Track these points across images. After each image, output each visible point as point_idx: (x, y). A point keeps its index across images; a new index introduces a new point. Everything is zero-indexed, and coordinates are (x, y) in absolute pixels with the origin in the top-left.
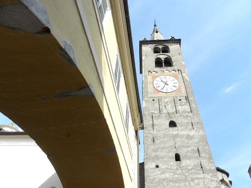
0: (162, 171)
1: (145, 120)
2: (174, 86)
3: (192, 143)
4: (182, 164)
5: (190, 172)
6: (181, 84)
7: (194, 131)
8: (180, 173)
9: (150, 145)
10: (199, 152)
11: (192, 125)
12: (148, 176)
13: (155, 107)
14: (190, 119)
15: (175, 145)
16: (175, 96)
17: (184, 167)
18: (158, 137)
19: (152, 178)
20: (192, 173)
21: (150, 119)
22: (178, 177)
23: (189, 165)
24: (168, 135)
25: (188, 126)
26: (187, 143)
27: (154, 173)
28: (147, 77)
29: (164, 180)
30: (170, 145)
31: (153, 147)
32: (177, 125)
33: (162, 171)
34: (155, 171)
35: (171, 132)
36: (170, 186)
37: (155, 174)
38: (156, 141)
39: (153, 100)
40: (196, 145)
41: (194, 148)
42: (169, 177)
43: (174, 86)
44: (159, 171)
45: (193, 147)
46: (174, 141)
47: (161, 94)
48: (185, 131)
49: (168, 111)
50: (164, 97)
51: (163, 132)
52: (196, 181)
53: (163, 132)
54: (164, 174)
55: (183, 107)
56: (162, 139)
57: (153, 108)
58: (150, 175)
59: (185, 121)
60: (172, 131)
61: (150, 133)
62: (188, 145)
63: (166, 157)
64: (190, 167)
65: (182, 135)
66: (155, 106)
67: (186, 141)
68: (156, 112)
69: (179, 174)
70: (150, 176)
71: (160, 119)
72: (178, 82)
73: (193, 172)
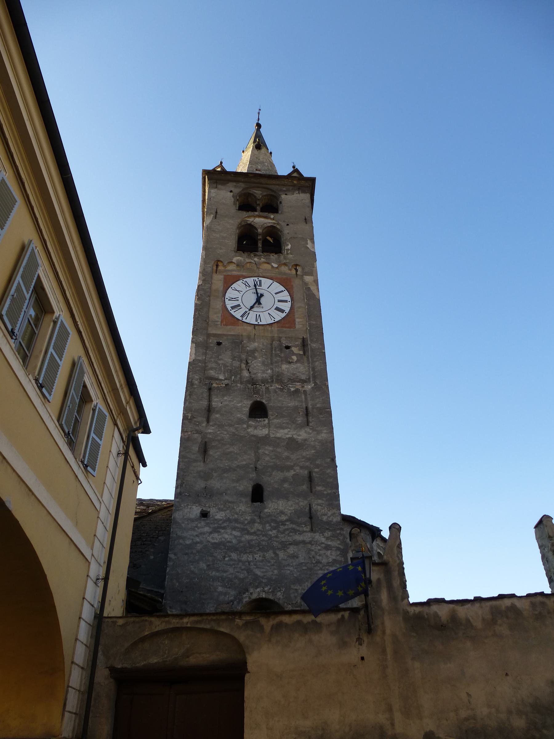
2: (277, 309)
3: (298, 459)
4: (266, 510)
5: (282, 528)
6: (297, 305)
7: (308, 429)
8: (258, 530)
12: (180, 537)
13: (220, 362)
14: (304, 400)
17: (269, 516)
19: (188, 542)
22: (252, 540)
23: (282, 513)
25: (296, 417)
26: (288, 458)
27: (194, 530)
28: (212, 277)
29: (216, 546)
30: (244, 463)
31: (200, 466)
33: (216, 525)
34: (197, 527)
36: (228, 560)
37: (195, 533)
38: (211, 452)
39: (219, 344)
40: (308, 464)
41: (301, 471)
44: (207, 525)
45: (298, 469)
47: (240, 327)
48: (286, 428)
50: (249, 337)
51: (232, 430)
52: (292, 550)
53: (232, 430)
54: (219, 532)
55: (293, 366)
57: (214, 365)
58: (185, 534)
60: (256, 428)
61: (198, 432)
62: (288, 463)
63: (229, 492)
64: (284, 518)
65: (279, 438)
66: (221, 359)
67: (286, 454)
68: (221, 377)
69: (254, 533)
70: (184, 538)
72: (289, 298)
73: (287, 529)
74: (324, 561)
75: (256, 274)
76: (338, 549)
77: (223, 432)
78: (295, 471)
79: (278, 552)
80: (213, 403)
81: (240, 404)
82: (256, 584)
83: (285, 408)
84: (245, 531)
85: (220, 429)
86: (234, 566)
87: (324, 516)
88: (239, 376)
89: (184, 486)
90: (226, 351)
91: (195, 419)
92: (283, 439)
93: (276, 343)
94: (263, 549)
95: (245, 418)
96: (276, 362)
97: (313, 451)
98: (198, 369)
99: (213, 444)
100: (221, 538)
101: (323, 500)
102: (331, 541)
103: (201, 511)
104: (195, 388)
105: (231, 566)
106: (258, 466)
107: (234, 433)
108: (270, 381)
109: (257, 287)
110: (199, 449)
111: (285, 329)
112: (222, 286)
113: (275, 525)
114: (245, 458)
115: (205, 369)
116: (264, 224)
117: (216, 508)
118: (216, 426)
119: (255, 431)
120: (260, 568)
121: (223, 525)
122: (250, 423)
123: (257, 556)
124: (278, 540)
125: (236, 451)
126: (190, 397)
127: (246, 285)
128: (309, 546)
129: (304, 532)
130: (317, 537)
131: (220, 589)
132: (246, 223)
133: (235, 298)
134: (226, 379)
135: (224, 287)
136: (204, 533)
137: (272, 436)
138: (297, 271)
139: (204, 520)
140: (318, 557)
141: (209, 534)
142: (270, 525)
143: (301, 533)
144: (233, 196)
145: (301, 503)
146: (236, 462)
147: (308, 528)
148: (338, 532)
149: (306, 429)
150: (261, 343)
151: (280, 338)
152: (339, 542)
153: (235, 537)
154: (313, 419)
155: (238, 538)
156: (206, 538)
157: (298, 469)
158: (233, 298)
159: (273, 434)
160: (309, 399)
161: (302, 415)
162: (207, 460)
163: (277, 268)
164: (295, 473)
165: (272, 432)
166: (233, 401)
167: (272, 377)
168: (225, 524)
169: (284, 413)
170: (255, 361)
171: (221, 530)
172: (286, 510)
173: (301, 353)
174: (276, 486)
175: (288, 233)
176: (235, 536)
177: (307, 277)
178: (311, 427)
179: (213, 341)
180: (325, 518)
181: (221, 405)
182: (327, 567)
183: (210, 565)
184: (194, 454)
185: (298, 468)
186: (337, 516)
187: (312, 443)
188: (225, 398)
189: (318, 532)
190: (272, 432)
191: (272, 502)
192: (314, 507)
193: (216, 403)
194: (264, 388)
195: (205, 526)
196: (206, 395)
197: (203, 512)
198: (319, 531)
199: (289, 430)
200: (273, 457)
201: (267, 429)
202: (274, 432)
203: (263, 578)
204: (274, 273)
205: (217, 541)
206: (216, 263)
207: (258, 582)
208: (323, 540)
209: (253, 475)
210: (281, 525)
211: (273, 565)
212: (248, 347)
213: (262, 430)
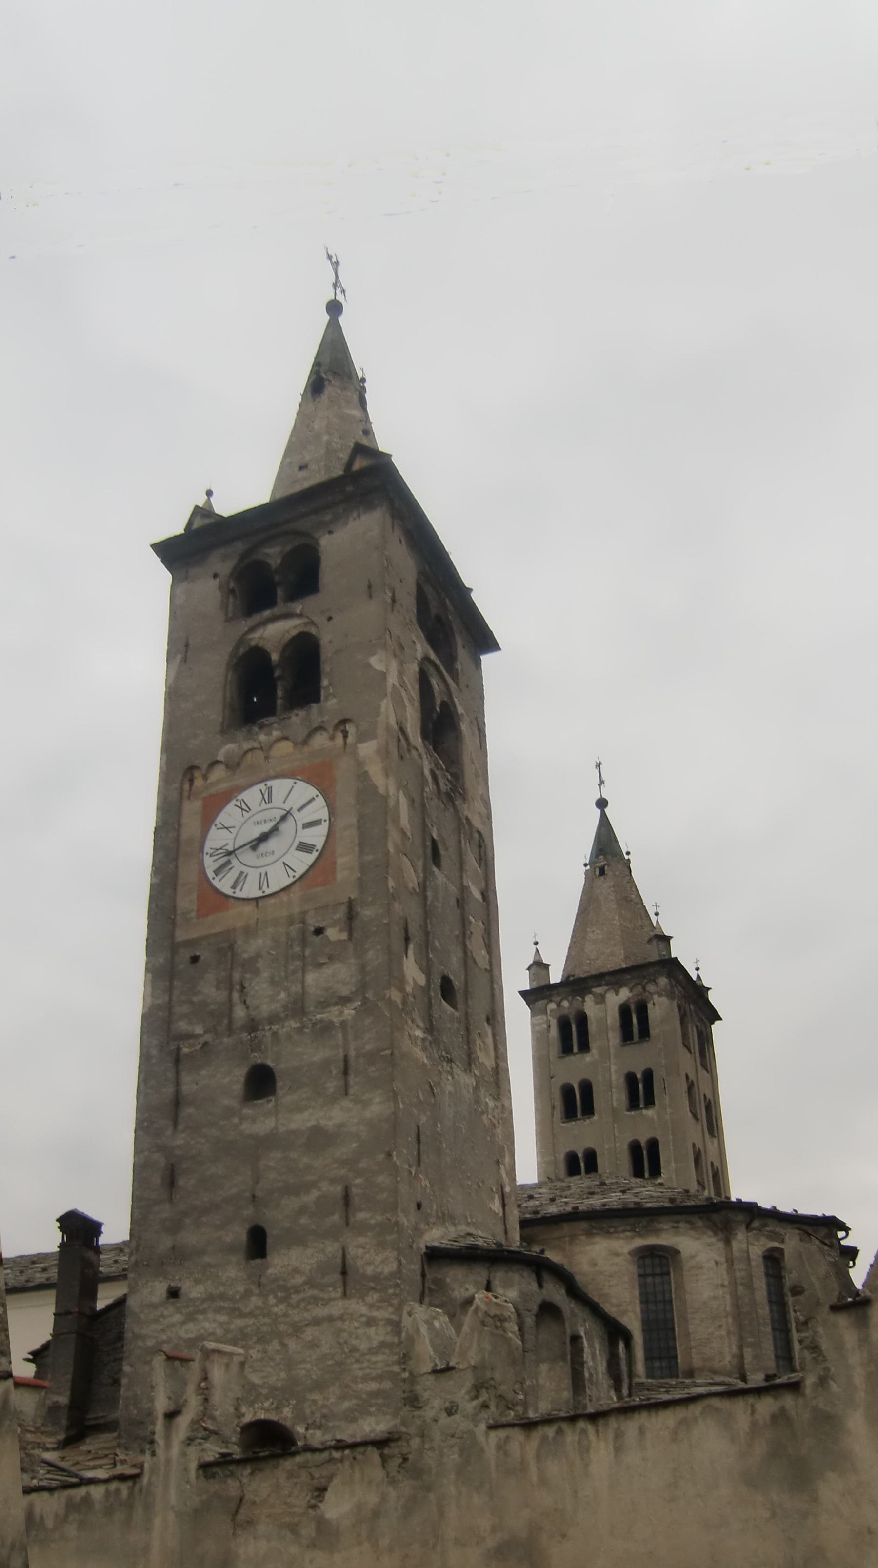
4: (270, 1271)
5: (295, 1298)
8: (257, 1307)
13: (195, 999)
16: (296, 910)
17: (276, 1280)
20: (299, 1302)
22: (246, 1327)
23: (296, 1271)
30: (234, 1191)
31: (165, 1211)
32: (279, 1084)
33: (191, 1309)
38: (181, 1182)
40: (343, 1172)
41: (331, 1189)
43: (305, 847)
45: (325, 1186)
49: (253, 1013)
52: (309, 1333)
57: (185, 1009)
58: (145, 1331)
60: (254, 1120)
62: (309, 1178)
64: (299, 1280)
67: (305, 1160)
68: (199, 1030)
69: (251, 1314)
70: (143, 1337)
73: (303, 1300)
74: (364, 1346)
76: (389, 1322)
79: (287, 1341)
84: (236, 1312)
88: (226, 1021)
89: (141, 1249)
91: (155, 1126)
93: (294, 930)
94: (262, 1339)
96: (294, 972)
97: (355, 1145)
102: (377, 1310)
106: (259, 1194)
113: (283, 1294)
115: (169, 1022)
121: (201, 1308)
125: (220, 1172)
127: (242, 809)
128: (339, 1324)
129: (330, 1300)
133: (221, 849)
138: (345, 735)
140: (354, 1342)
142: (276, 1297)
143: (327, 1302)
147: (340, 1290)
148: (391, 1291)
151: (305, 913)
152: (390, 1310)
153: (221, 1324)
155: (225, 1326)
157: (325, 1186)
164: (320, 1193)
167: (285, 1007)
168: (205, 1306)
171: (198, 1316)
178: (352, 1097)
179: (185, 955)
180: (369, 1270)
182: (367, 1357)
192: (352, 1251)
194: (268, 1034)
196: (171, 1075)
198: (358, 1295)
199: (311, 1111)
201: (274, 1119)
208: (364, 1310)
209: (249, 1212)
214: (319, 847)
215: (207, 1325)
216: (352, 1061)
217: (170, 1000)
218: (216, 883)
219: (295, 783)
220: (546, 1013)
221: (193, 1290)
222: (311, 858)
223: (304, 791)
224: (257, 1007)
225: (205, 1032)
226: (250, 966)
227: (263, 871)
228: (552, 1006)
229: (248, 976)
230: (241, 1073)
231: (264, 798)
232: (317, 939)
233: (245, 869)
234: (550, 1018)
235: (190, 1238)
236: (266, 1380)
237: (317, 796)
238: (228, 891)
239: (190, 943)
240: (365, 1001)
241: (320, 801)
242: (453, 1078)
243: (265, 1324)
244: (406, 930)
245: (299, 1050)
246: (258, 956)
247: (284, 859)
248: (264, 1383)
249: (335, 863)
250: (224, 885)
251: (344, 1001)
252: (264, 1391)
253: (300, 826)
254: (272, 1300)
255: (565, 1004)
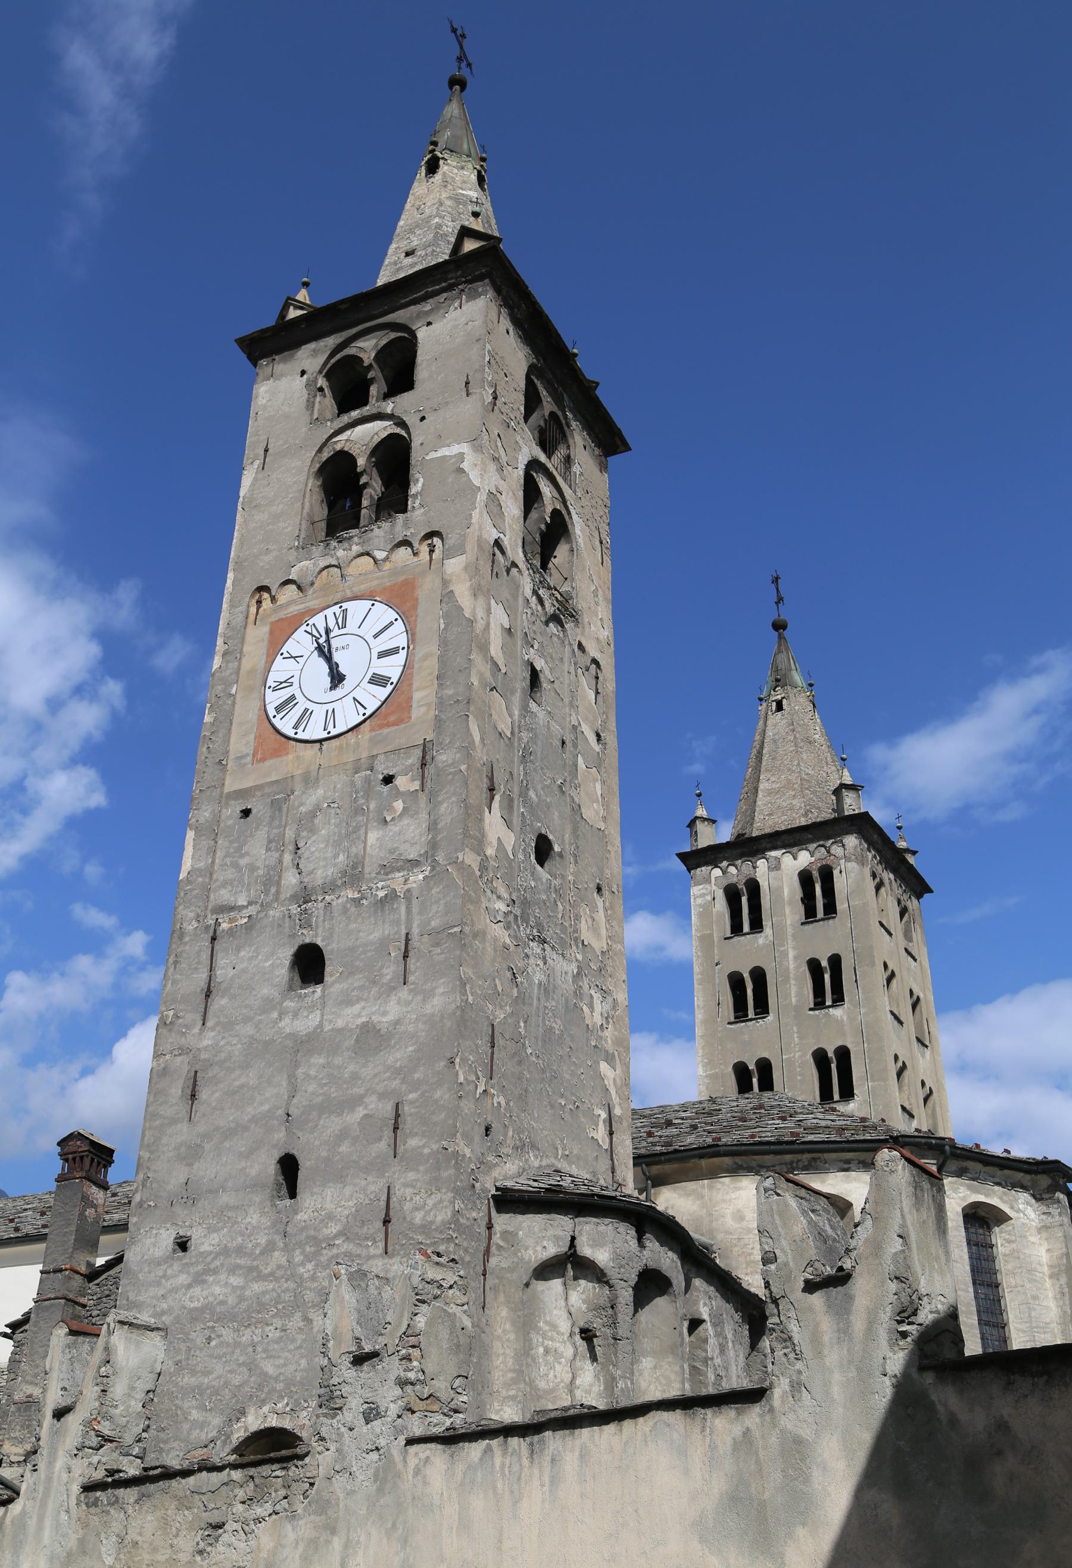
0: (200, 1267)
1: (176, 963)
3: (375, 1075)
4: (299, 1217)
7: (404, 993)
8: (279, 1267)
9: (174, 1121)
10: (396, 1129)
11: (406, 957)
13: (243, 862)
15: (288, 1105)
16: (365, 754)
17: (305, 1228)
18: (215, 1070)
21: (199, 953)
22: (264, 1293)
23: (330, 1217)
24: (268, 1044)
25: (382, 967)
26: (355, 1076)
27: (158, 1284)
29: (195, 1315)
30: (266, 1107)
31: (183, 1133)
32: (328, 969)
33: (200, 1267)
35: (287, 1020)
37: (162, 1292)
38: (203, 1094)
40: (395, 1083)
42: (221, 1297)
43: (378, 680)
46: (292, 1077)
48: (359, 999)
49: (306, 880)
51: (249, 1030)
53: (249, 1030)
54: (204, 1282)
55: (394, 828)
56: (233, 1076)
57: (230, 874)
59: (375, 936)
60: (296, 1015)
61: (183, 1051)
62: (357, 1091)
63: (230, 1184)
64: (333, 1229)
65: (340, 1031)
66: (247, 854)
68: (242, 901)
71: (250, 946)
75: (338, 597)
77: (231, 1039)
78: (366, 1108)
79: (311, 1315)
80: (219, 972)
81: (270, 962)
82: (263, 1396)
83: (361, 949)
84: (253, 1273)
85: (226, 1035)
86: (224, 1359)
87: (417, 1213)
89: (148, 1185)
90: (257, 828)
91: (180, 1021)
92: (351, 1030)
95: (275, 993)
97: (411, 1049)
98: (195, 892)
99: (210, 1075)
100: (207, 1297)
101: (418, 1171)
103: (176, 1238)
104: (186, 944)
105: (219, 1357)
107: (251, 1037)
108: (339, 883)
109: (336, 632)
110: (182, 1091)
111: (386, 731)
112: (265, 656)
113: (313, 1249)
114: (267, 1095)
116: (372, 438)
117: (204, 1226)
118: (218, 1028)
119: (296, 1022)
120: (275, 1357)
121: (212, 1266)
122: (284, 1004)
123: (272, 1333)
124: (316, 1284)
126: (175, 967)
130: (395, 1267)
131: (195, 1414)
132: (332, 453)
133: (285, 682)
134: (250, 903)
135: (268, 655)
136: (175, 1290)
137: (327, 1027)
139: (180, 1259)
141: (186, 1290)
144: (307, 385)
145: (372, 1188)
146: (250, 1109)
149: (400, 995)
150: (332, 786)
154: (418, 964)
156: (180, 1300)
157: (372, 1102)
158: (281, 683)
159: (331, 1021)
160: (415, 910)
161: (395, 957)
162: (195, 1115)
163: (387, 559)
165: (329, 1017)
166: (257, 957)
167: (344, 873)
169: (357, 963)
170: (313, 838)
172: (339, 1209)
173: (416, 785)
174: (324, 1154)
175: (422, 444)
176: (233, 1287)
177: (453, 561)
178: (412, 987)
181: (232, 972)
183: (180, 1361)
184: (172, 1106)
185: (374, 1098)
186: (446, 1207)
187: (411, 1028)
188: (242, 954)
189: (398, 1254)
190: (329, 1017)
191: (312, 1194)
192: (398, 1192)
193: (223, 971)
194: (321, 905)
195: (180, 1271)
196: (205, 956)
197: (179, 1241)
199: (363, 1004)
200: (324, 1082)
201: (318, 1012)
202: (330, 1017)
203: (276, 1379)
204: (378, 578)
205: (200, 1305)
206: (257, 597)
207: (266, 1390)
209: (280, 1135)
210: (325, 1248)
211: (300, 1347)
212: (302, 804)
213: (307, 1017)
214: (394, 680)
215: (217, 1290)
216: (415, 942)
217: (213, 862)
218: (276, 722)
219: (373, 605)
220: (710, 882)
221: (204, 1242)
222: (383, 692)
223: (383, 614)
224: (312, 872)
225: (250, 903)
226: (308, 822)
227: (330, 707)
228: (717, 872)
229: (304, 834)
230: (286, 954)
231: (337, 623)
232: (386, 789)
233: (311, 706)
234: (714, 887)
235: (206, 1170)
236: (282, 1371)
237: (396, 620)
238: (290, 733)
239: (240, 794)
240: (434, 865)
241: (399, 626)
242: (545, 964)
243: (287, 1290)
244: (491, 779)
245: (353, 926)
246: (318, 808)
247: (356, 694)
248: (281, 1374)
249: (411, 698)
250: (285, 726)
251: (414, 863)
252: (280, 1386)
253: (375, 655)
254: (298, 1258)
255: (732, 870)
